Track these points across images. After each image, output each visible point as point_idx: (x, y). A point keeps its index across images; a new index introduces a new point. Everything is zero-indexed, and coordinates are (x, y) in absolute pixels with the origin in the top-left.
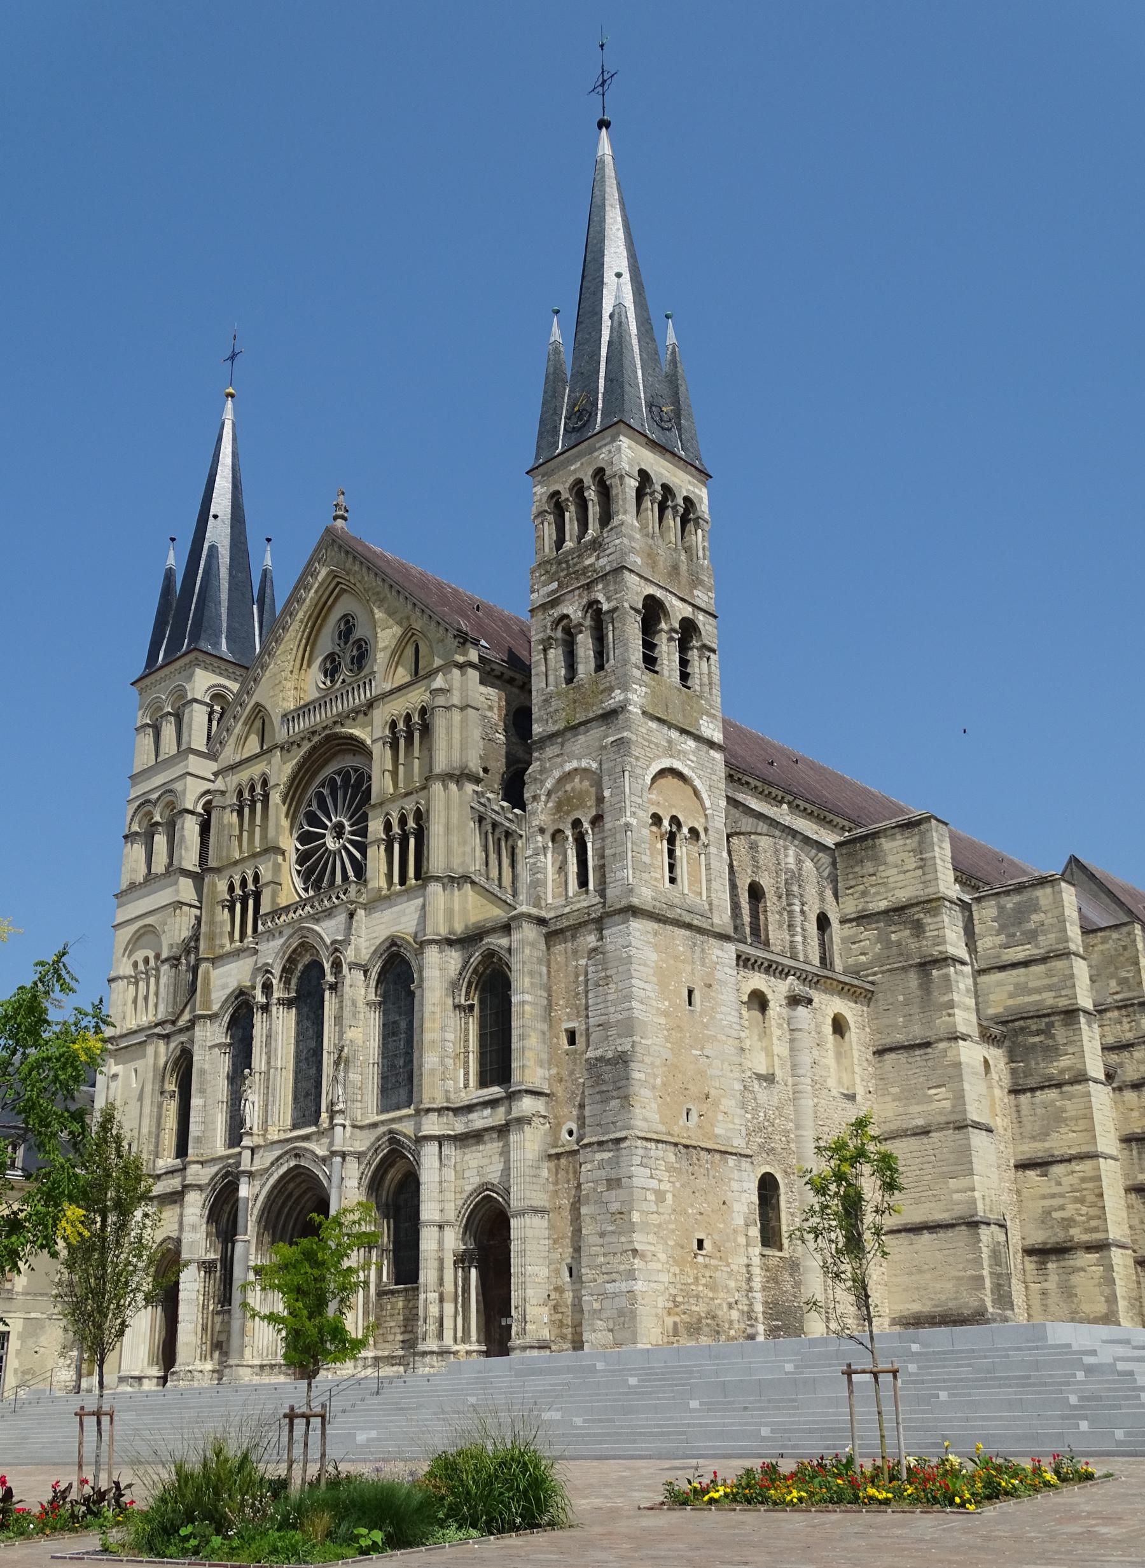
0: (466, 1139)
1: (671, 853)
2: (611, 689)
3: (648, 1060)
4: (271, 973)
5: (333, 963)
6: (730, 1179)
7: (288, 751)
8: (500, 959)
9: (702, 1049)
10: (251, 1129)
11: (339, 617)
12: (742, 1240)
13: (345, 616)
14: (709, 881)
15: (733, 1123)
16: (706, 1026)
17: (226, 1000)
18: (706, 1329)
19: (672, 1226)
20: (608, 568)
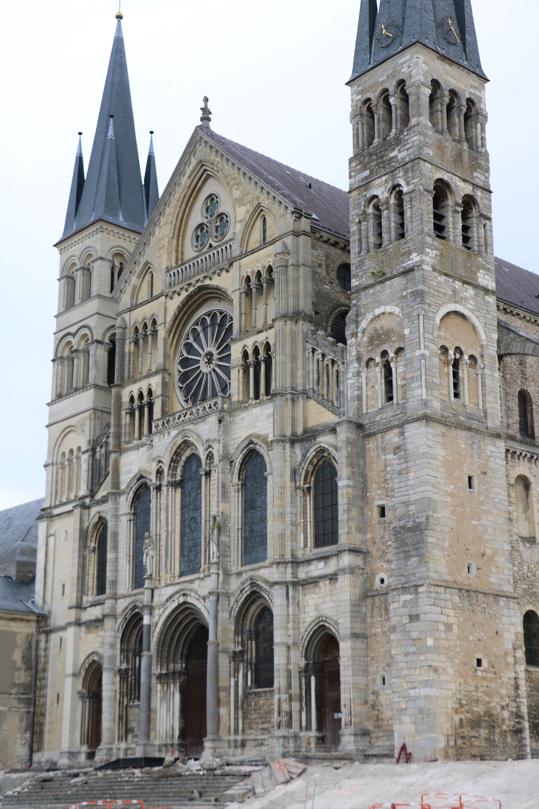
1: (456, 375)
2: (410, 253)
3: (438, 528)
5: (208, 456)
6: (501, 615)
7: (171, 298)
8: (329, 454)
9: (479, 520)
10: (151, 575)
12: (511, 660)
13: (210, 195)
14: (484, 395)
15: (503, 574)
16: (482, 503)
17: (131, 481)
18: (484, 724)
19: (458, 649)
20: (407, 159)
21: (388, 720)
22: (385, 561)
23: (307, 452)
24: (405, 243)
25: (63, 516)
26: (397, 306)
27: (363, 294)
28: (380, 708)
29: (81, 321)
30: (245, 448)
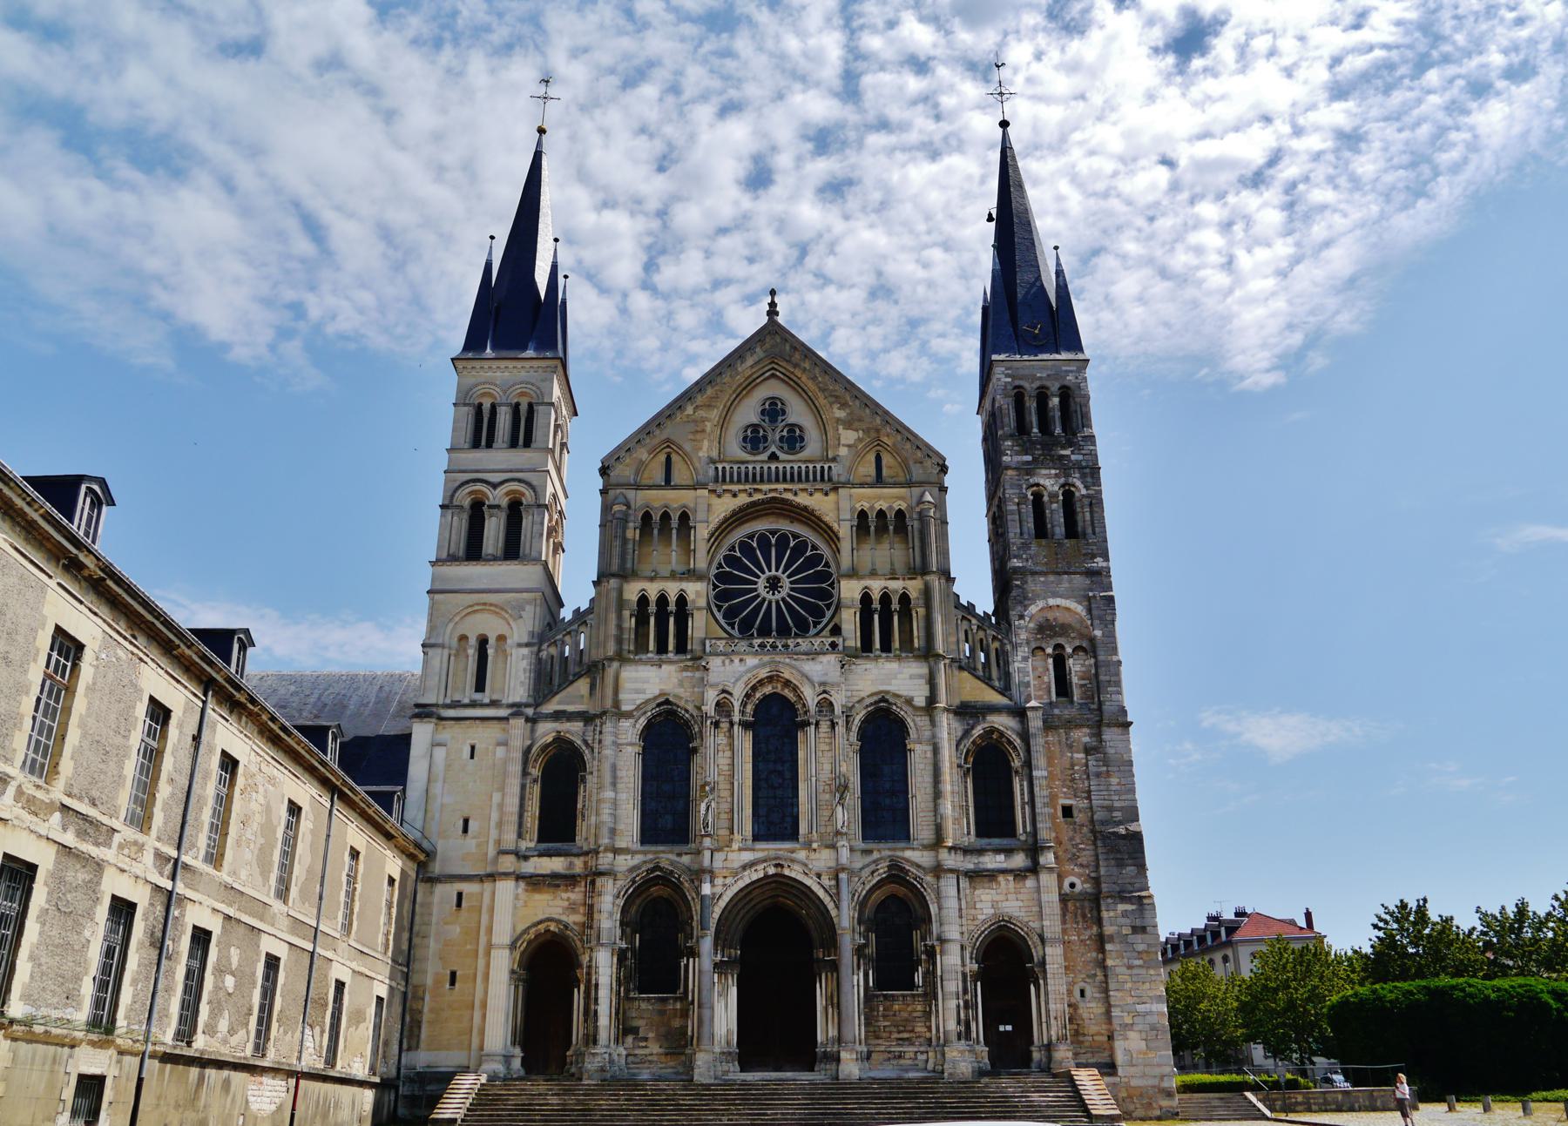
2: (1093, 556)
4: (731, 694)
23: (973, 728)
24: (1088, 544)
25: (468, 722)
26: (1080, 603)
27: (1030, 579)
28: (1080, 1022)
30: (871, 704)
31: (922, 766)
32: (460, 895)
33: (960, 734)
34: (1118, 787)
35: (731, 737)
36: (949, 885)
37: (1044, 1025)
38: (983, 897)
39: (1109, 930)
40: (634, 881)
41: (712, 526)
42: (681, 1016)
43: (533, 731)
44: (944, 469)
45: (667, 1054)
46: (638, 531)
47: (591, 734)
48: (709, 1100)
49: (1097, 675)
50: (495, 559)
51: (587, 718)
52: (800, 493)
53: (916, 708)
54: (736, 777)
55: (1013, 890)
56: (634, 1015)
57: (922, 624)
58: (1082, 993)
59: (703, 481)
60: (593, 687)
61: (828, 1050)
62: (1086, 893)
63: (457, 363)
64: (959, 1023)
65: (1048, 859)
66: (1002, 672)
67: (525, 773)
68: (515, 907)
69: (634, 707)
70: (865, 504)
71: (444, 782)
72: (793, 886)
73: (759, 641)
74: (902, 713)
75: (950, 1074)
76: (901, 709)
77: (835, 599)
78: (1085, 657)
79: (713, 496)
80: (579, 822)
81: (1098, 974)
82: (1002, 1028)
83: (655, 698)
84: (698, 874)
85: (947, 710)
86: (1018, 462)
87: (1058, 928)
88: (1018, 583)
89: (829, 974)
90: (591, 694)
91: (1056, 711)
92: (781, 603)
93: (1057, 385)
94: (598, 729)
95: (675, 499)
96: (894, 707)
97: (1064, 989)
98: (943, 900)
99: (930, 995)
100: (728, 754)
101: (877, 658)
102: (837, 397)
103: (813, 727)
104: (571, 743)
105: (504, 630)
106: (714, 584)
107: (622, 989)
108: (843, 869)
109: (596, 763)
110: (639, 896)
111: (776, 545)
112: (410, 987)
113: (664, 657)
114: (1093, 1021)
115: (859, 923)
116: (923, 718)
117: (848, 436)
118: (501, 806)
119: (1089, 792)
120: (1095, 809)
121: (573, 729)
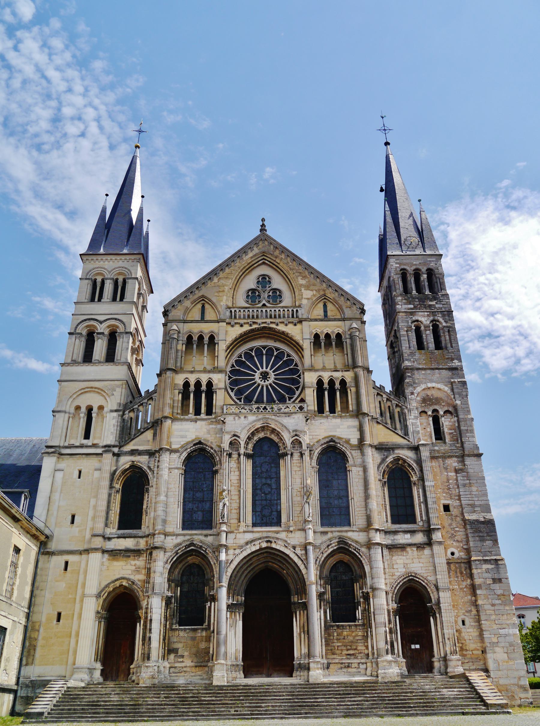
0: (392, 548)
2: (452, 359)
4: (239, 437)
11: (262, 273)
21: (472, 651)
22: (454, 541)
23: (387, 457)
24: (449, 353)
25: (78, 456)
26: (446, 386)
29: (111, 314)
30: (325, 443)
31: (357, 480)
32: (67, 563)
33: (379, 461)
34: (477, 493)
35: (239, 463)
36: (377, 553)
37: (441, 644)
38: (398, 561)
39: (478, 581)
40: (177, 553)
41: (228, 342)
42: (206, 641)
43: (117, 461)
44: (363, 312)
45: (196, 667)
46: (184, 346)
47: (153, 462)
48: (222, 697)
49: (459, 426)
50: (100, 362)
51: (151, 454)
52: (280, 324)
53: (352, 446)
54: (242, 487)
55: (416, 556)
56: (175, 641)
57: (354, 396)
58: (463, 623)
59: (223, 318)
60: (155, 435)
61: (302, 662)
62: (462, 558)
63: (83, 257)
64: (386, 643)
65: (437, 536)
66: (402, 425)
67: (111, 487)
68: (101, 570)
69: (180, 446)
70: (318, 330)
71: (61, 493)
72: (278, 555)
73: (256, 406)
74: (344, 448)
75: (383, 678)
76: (343, 446)
77: (301, 384)
78: (451, 417)
79: (229, 326)
80: (144, 517)
81: (473, 610)
82: (413, 647)
83: (193, 441)
84: (217, 549)
85: (371, 446)
86: (405, 308)
87: (447, 580)
88: (409, 374)
89: (302, 612)
90: (154, 439)
91: (436, 448)
92: (269, 387)
93: (425, 268)
94: (157, 459)
95: (206, 328)
96: (339, 445)
97: (453, 619)
98: (373, 563)
99: (367, 625)
100: (237, 473)
101: (327, 417)
102: (300, 273)
103: (289, 456)
104: (140, 468)
105: (102, 402)
106: (229, 377)
107: (168, 623)
108: (310, 543)
109: (155, 480)
110: (180, 562)
111: (266, 354)
112: (30, 623)
113: (198, 417)
114: (472, 641)
115: (320, 578)
116: (356, 451)
117: (307, 294)
118: (95, 507)
119: (459, 496)
120: (464, 506)
121: (142, 461)
